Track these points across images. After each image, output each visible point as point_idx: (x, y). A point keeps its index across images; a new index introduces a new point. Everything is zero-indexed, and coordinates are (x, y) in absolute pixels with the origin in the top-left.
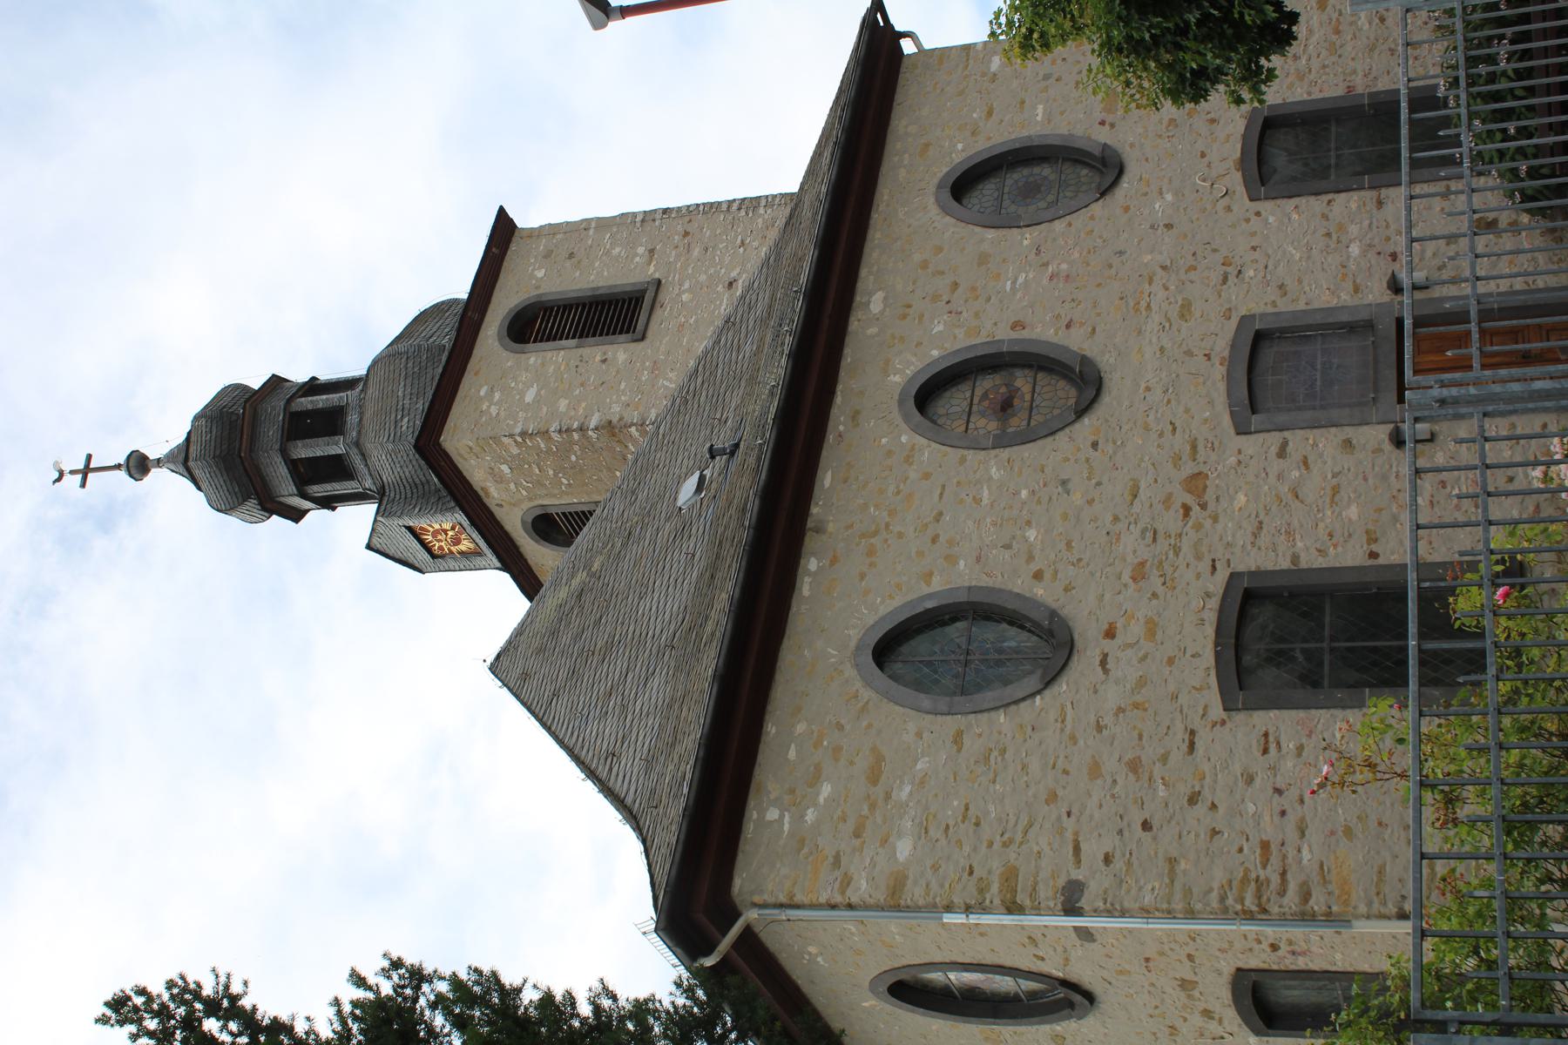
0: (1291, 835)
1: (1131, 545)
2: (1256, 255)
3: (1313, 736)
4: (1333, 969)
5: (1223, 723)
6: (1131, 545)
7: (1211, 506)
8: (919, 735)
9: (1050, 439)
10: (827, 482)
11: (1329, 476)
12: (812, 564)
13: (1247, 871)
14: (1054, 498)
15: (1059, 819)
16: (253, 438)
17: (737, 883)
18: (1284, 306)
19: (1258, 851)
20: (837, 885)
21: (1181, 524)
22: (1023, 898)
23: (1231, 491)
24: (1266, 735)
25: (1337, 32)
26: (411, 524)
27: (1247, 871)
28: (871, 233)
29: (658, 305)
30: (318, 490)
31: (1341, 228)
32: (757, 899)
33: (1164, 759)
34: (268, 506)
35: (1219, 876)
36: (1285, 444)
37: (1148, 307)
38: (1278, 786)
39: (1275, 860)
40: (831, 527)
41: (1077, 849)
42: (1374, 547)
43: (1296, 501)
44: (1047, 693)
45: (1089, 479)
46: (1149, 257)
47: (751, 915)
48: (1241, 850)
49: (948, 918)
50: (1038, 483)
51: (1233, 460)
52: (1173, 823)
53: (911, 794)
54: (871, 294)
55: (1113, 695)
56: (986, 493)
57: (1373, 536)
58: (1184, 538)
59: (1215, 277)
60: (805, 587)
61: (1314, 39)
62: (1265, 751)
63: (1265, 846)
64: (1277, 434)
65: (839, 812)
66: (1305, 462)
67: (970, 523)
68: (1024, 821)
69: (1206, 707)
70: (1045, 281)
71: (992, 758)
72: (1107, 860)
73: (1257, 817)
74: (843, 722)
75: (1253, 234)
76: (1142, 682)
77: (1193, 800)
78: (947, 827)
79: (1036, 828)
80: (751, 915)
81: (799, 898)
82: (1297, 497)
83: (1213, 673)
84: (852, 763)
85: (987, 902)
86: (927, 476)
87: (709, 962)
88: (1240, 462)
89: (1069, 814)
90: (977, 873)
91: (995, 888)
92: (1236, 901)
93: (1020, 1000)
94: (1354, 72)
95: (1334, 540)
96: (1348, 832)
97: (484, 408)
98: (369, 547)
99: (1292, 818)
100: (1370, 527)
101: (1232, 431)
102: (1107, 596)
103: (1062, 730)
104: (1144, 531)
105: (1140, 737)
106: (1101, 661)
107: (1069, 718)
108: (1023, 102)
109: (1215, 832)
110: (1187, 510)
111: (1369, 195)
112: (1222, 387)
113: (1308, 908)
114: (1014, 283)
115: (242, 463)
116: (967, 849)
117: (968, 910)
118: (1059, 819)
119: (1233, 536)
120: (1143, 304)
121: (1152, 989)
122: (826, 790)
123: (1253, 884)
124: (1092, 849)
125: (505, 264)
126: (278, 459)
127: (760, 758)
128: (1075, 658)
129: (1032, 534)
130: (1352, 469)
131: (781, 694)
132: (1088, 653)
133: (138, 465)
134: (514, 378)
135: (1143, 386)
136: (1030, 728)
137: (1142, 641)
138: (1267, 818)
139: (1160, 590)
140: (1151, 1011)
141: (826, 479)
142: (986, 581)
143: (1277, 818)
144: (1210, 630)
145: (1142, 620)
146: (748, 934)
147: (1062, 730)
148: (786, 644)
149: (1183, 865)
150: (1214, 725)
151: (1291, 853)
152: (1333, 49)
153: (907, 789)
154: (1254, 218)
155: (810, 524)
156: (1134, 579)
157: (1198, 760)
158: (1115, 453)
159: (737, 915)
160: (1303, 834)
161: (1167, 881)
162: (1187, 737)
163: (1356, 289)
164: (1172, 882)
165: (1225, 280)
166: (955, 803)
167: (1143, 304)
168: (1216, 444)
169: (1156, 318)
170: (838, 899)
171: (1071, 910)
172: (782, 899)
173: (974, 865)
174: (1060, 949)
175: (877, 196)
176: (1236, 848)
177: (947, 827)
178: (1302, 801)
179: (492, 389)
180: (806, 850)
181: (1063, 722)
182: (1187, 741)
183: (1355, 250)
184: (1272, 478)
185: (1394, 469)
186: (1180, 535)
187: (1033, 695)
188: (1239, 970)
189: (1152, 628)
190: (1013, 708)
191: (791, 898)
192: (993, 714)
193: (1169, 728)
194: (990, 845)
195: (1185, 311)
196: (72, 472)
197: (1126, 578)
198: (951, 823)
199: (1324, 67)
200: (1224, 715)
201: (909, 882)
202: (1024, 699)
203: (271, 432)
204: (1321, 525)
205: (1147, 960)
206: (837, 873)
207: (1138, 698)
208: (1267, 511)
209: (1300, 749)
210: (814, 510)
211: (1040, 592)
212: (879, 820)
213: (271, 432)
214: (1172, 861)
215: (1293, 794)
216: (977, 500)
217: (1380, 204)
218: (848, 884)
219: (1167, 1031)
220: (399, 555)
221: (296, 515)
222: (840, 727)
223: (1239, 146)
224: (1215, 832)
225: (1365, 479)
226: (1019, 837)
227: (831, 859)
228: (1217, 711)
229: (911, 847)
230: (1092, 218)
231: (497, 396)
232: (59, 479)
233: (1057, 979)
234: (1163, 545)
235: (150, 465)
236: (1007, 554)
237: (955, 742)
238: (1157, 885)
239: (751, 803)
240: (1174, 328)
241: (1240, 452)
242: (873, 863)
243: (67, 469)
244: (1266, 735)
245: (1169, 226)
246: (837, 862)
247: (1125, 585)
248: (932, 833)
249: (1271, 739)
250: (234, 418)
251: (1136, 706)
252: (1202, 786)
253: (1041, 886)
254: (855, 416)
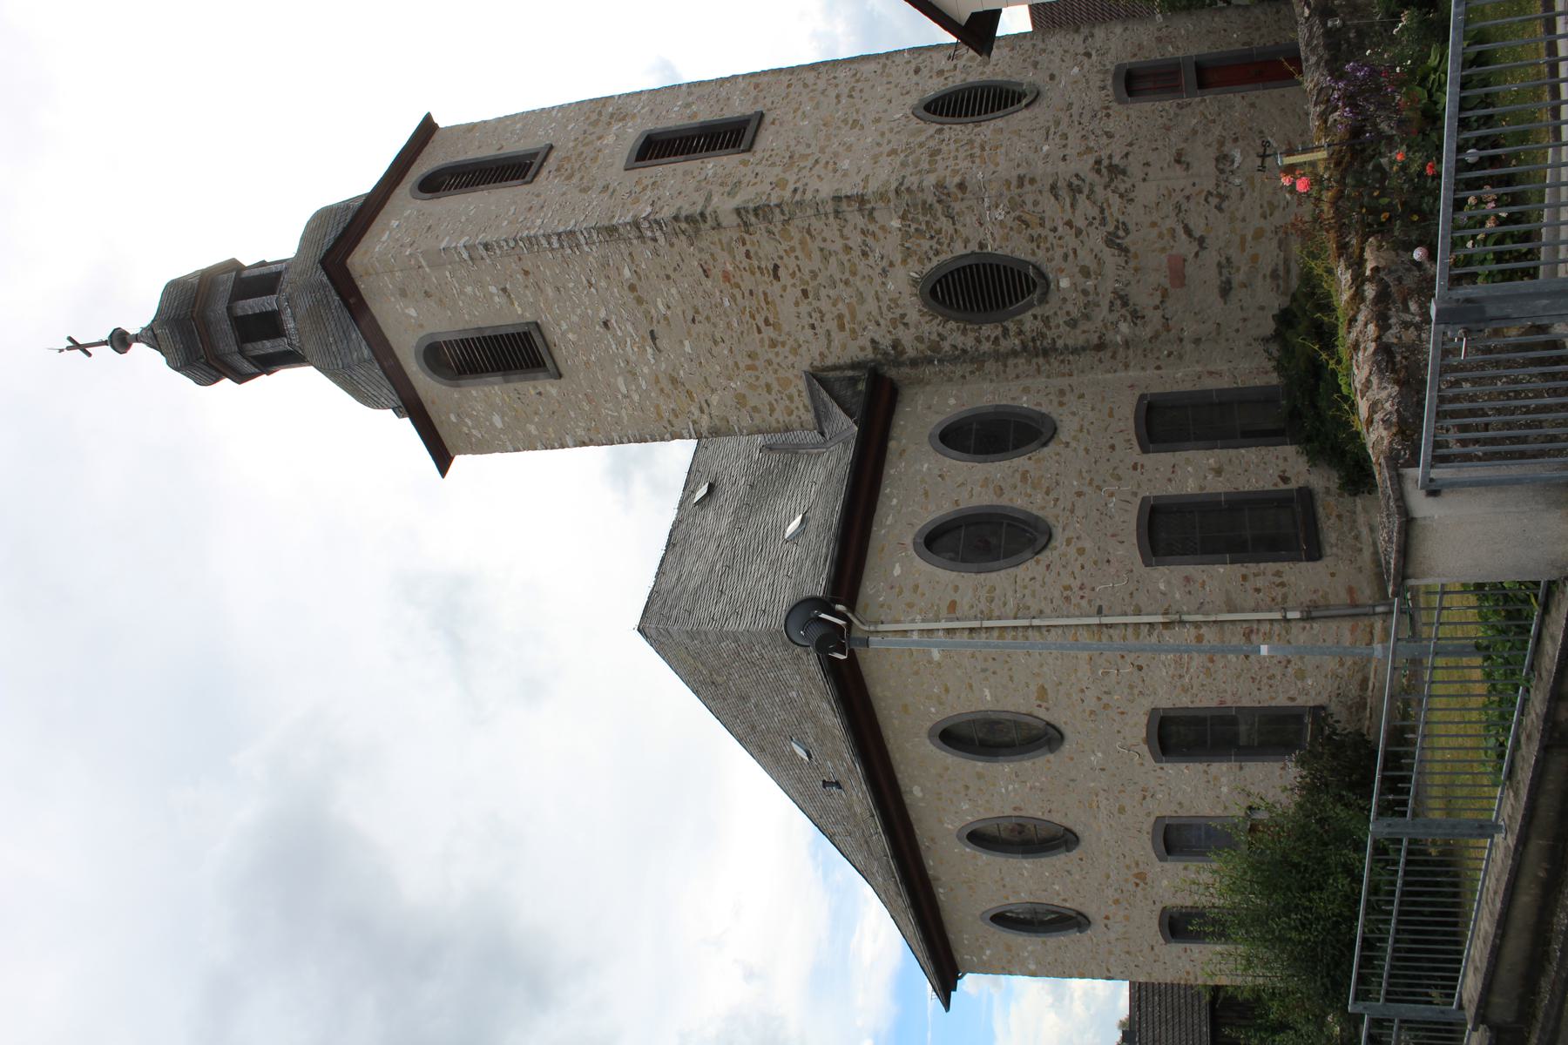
1: (1110, 892)
2: (1163, 788)
7: (1150, 882)
18: (1182, 813)
25: (1212, 661)
28: (891, 755)
29: (552, 346)
31: (1216, 778)
37: (1098, 807)
59: (1138, 797)
61: (1194, 664)
70: (1027, 790)
75: (1160, 778)
94: (1225, 691)
108: (971, 686)
111: (1234, 765)
120: (1094, 804)
129: (1057, 887)
133: (120, 341)
135: (1103, 839)
141: (930, 863)
148: (942, 913)
152: (1208, 672)
154: (1159, 770)
163: (1226, 808)
165: (1144, 798)
167: (1094, 804)
183: (1225, 790)
189: (1127, 918)
195: (1122, 810)
199: (1203, 685)
211: (1068, 905)
217: (1241, 768)
223: (1144, 730)
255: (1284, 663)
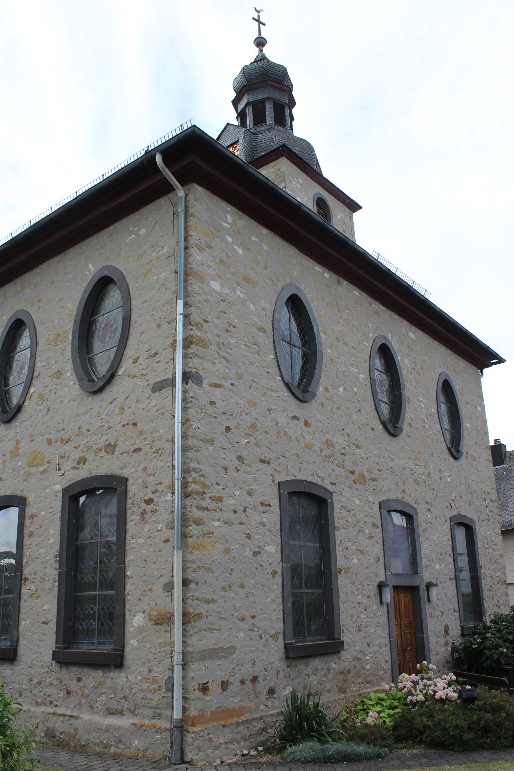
0: (228, 515)
3: (269, 533)
4: (128, 538)
5: (273, 481)
6: (340, 441)
7: (355, 486)
8: (263, 309)
9: (374, 407)
10: (355, 292)
11: (367, 549)
12: (327, 275)
13: (208, 487)
14: (354, 405)
15: (230, 378)
16: (275, 88)
17: (199, 189)
19: (218, 495)
20: (199, 243)
21: (348, 469)
22: (193, 349)
23: (360, 497)
24: (269, 505)
26: (239, 142)
27: (208, 487)
30: (249, 112)
32: (191, 197)
33: (257, 445)
34: (244, 89)
35: (206, 469)
36: (377, 527)
37: (417, 465)
38: (247, 510)
39: (213, 505)
40: (340, 288)
41: (217, 386)
42: (343, 572)
43: (357, 531)
44: (282, 384)
45: (362, 424)
46: (432, 467)
47: (181, 192)
48: (218, 484)
49: (180, 303)
50: (359, 398)
51: (371, 499)
52: (230, 445)
53: (239, 297)
54: (414, 333)
55: (283, 420)
56: (355, 370)
57: (347, 571)
58: (343, 470)
60: (319, 269)
62: (262, 504)
63: (220, 499)
64: (380, 523)
65: (231, 255)
66: (371, 537)
67: (344, 359)
68: (230, 358)
69: (280, 472)
70: (422, 416)
71: (255, 346)
72: (212, 403)
73: (233, 496)
74: (268, 270)
76: (289, 437)
77: (240, 458)
78: (226, 313)
79: (226, 364)
80: (181, 192)
81: (192, 221)
82: (359, 532)
83: (293, 478)
84: (252, 269)
85: (191, 327)
86: (359, 342)
87: (159, 159)
88: (370, 503)
89: (232, 384)
90: (204, 324)
91: (198, 333)
92: (194, 478)
93: (88, 353)
95: (345, 550)
96: (227, 551)
97: (295, 179)
98: (228, 124)
99: (232, 516)
100: (351, 569)
101: (380, 500)
102: (320, 425)
103: (268, 389)
104: (344, 448)
105: (266, 432)
106: (296, 416)
107: (273, 394)
109: (226, 469)
110: (353, 473)
112: (394, 497)
113: (191, 523)
114: (421, 401)
115: (265, 81)
116: (216, 321)
117: (186, 316)
118: (230, 378)
119: (345, 496)
121: (106, 427)
122: (240, 251)
123: (202, 490)
124: (217, 394)
125: (342, 204)
126: (265, 96)
127: (252, 221)
128: (297, 402)
130: (370, 561)
131: (278, 242)
132: (299, 410)
133: (260, 43)
134: (305, 195)
136: (268, 371)
137: (304, 440)
138: (233, 502)
139: (324, 454)
140: (84, 427)
142: (325, 361)
143: (233, 508)
144: (310, 479)
145: (312, 442)
146: (169, 189)
147: (268, 389)
149: (211, 448)
150: (273, 476)
151: (218, 515)
153: (241, 296)
155: (341, 279)
156: (327, 441)
157: (257, 464)
158: (371, 439)
159: (183, 185)
160: (226, 523)
161: (203, 437)
162: (267, 459)
164: (202, 440)
166: (236, 321)
168: (376, 491)
169: (414, 467)
170: (192, 242)
171: (186, 377)
172: (191, 211)
173: (208, 324)
174: (145, 372)
175: (441, 345)
176: (219, 482)
177: (226, 313)
178: (241, 524)
179: (301, 184)
180: (214, 231)
181: (271, 390)
182: (265, 459)
184: (365, 519)
185: (371, 583)
186: (344, 468)
187: (282, 376)
188: (127, 479)
189: (309, 446)
190: (276, 364)
191: (192, 215)
192: (273, 352)
193: (270, 449)
194: (218, 336)
196: (259, 16)
197: (328, 436)
198: (227, 315)
200: (277, 482)
201: (200, 284)
202: (280, 370)
203: (277, 95)
204: (349, 543)
205: (135, 424)
206: (204, 245)
207: (282, 434)
208: (354, 515)
209: (263, 524)
210: (345, 283)
211: (321, 389)
212: (228, 276)
213: (277, 95)
214: (211, 442)
215: (244, 520)
216: (352, 365)
218: (199, 249)
219: (67, 437)
220: (222, 137)
221: (235, 103)
222: (266, 268)
224: (226, 469)
225: (367, 568)
226: (222, 353)
227: (210, 243)
228: (279, 478)
229: (217, 290)
230: (441, 443)
231: (299, 186)
232: (256, 10)
233: (116, 371)
234: (340, 458)
235: (261, 47)
236: (333, 375)
237: (262, 328)
238: (201, 431)
239: (234, 209)
240: (411, 476)
241: (373, 503)
242: (209, 266)
243: (260, 14)
244: (269, 505)
245: (441, 478)
246: (209, 247)
247: (325, 435)
248: (222, 304)
249: (268, 508)
250: (283, 82)
251: (279, 432)
252: (246, 465)
253: (199, 361)
254: (376, 313)
255: (498, 604)
